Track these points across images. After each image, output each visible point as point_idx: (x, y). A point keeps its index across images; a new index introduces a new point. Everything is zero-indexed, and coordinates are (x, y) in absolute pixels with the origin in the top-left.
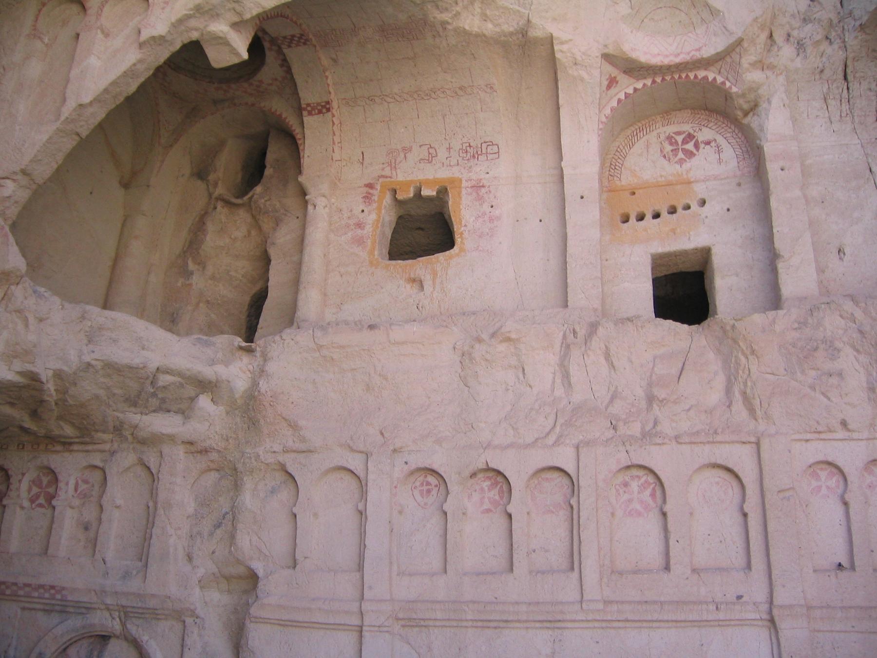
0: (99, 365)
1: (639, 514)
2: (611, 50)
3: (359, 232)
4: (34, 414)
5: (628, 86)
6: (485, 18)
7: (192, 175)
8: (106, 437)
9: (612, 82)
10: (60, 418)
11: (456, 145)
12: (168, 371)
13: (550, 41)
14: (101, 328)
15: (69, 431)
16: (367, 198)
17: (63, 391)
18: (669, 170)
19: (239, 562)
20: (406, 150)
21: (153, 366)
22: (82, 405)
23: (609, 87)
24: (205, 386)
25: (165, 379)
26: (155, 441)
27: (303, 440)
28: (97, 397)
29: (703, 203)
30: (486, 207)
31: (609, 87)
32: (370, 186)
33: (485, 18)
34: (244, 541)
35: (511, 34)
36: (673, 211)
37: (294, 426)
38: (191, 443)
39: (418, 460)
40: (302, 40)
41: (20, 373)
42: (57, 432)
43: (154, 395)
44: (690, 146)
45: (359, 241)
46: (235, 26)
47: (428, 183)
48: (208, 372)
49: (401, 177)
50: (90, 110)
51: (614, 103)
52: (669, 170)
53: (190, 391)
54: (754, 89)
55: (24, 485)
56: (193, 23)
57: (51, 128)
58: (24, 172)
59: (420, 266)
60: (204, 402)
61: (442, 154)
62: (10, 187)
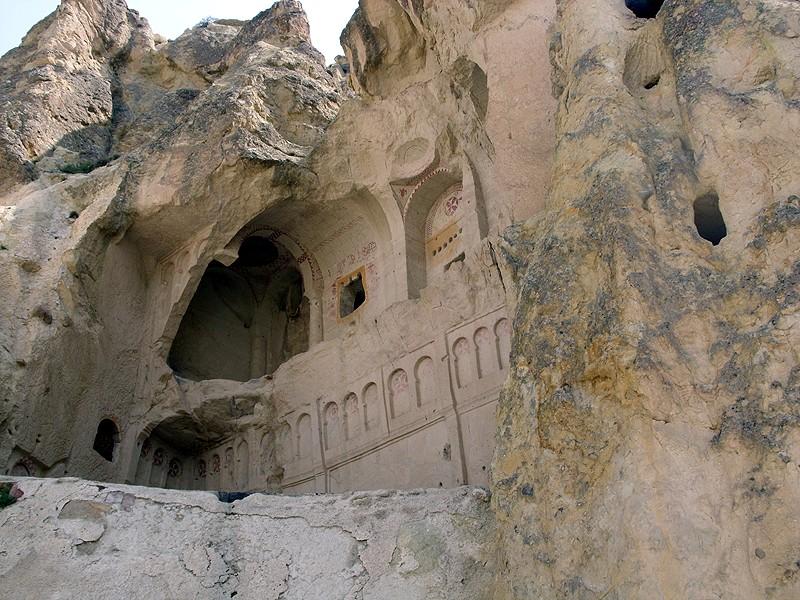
0: (209, 402)
1: (402, 390)
2: (392, 180)
3: (333, 309)
4: (198, 431)
5: (411, 191)
6: (337, 191)
7: (280, 310)
8: (230, 433)
9: (403, 192)
10: (209, 430)
11: (360, 250)
12: (238, 397)
13: (366, 188)
14: (208, 387)
15: (215, 435)
16: (334, 292)
17: (201, 417)
18: (448, 219)
19: (279, 467)
20: (344, 261)
21: (230, 397)
22: (213, 422)
23: (403, 195)
24: (256, 399)
25: (237, 401)
26: (243, 429)
27: (289, 408)
28: (216, 416)
29: (461, 231)
30: (375, 275)
31: (403, 195)
32: (334, 285)
33: (337, 191)
34: (279, 458)
35: (351, 192)
36: (451, 240)
37: (287, 404)
38: (255, 425)
39: (327, 401)
40: (278, 233)
41: (179, 412)
42: (211, 437)
43: (237, 409)
44: (455, 204)
45: (333, 314)
46: (227, 246)
47: (353, 273)
48: (254, 393)
49: (344, 276)
50: (180, 305)
51: (409, 201)
52: (448, 219)
53: (251, 403)
54: (456, 169)
55: (211, 465)
56: (207, 255)
57: (167, 318)
58: (163, 336)
59: (354, 316)
60: (258, 406)
61: (357, 257)
62: (160, 344)
